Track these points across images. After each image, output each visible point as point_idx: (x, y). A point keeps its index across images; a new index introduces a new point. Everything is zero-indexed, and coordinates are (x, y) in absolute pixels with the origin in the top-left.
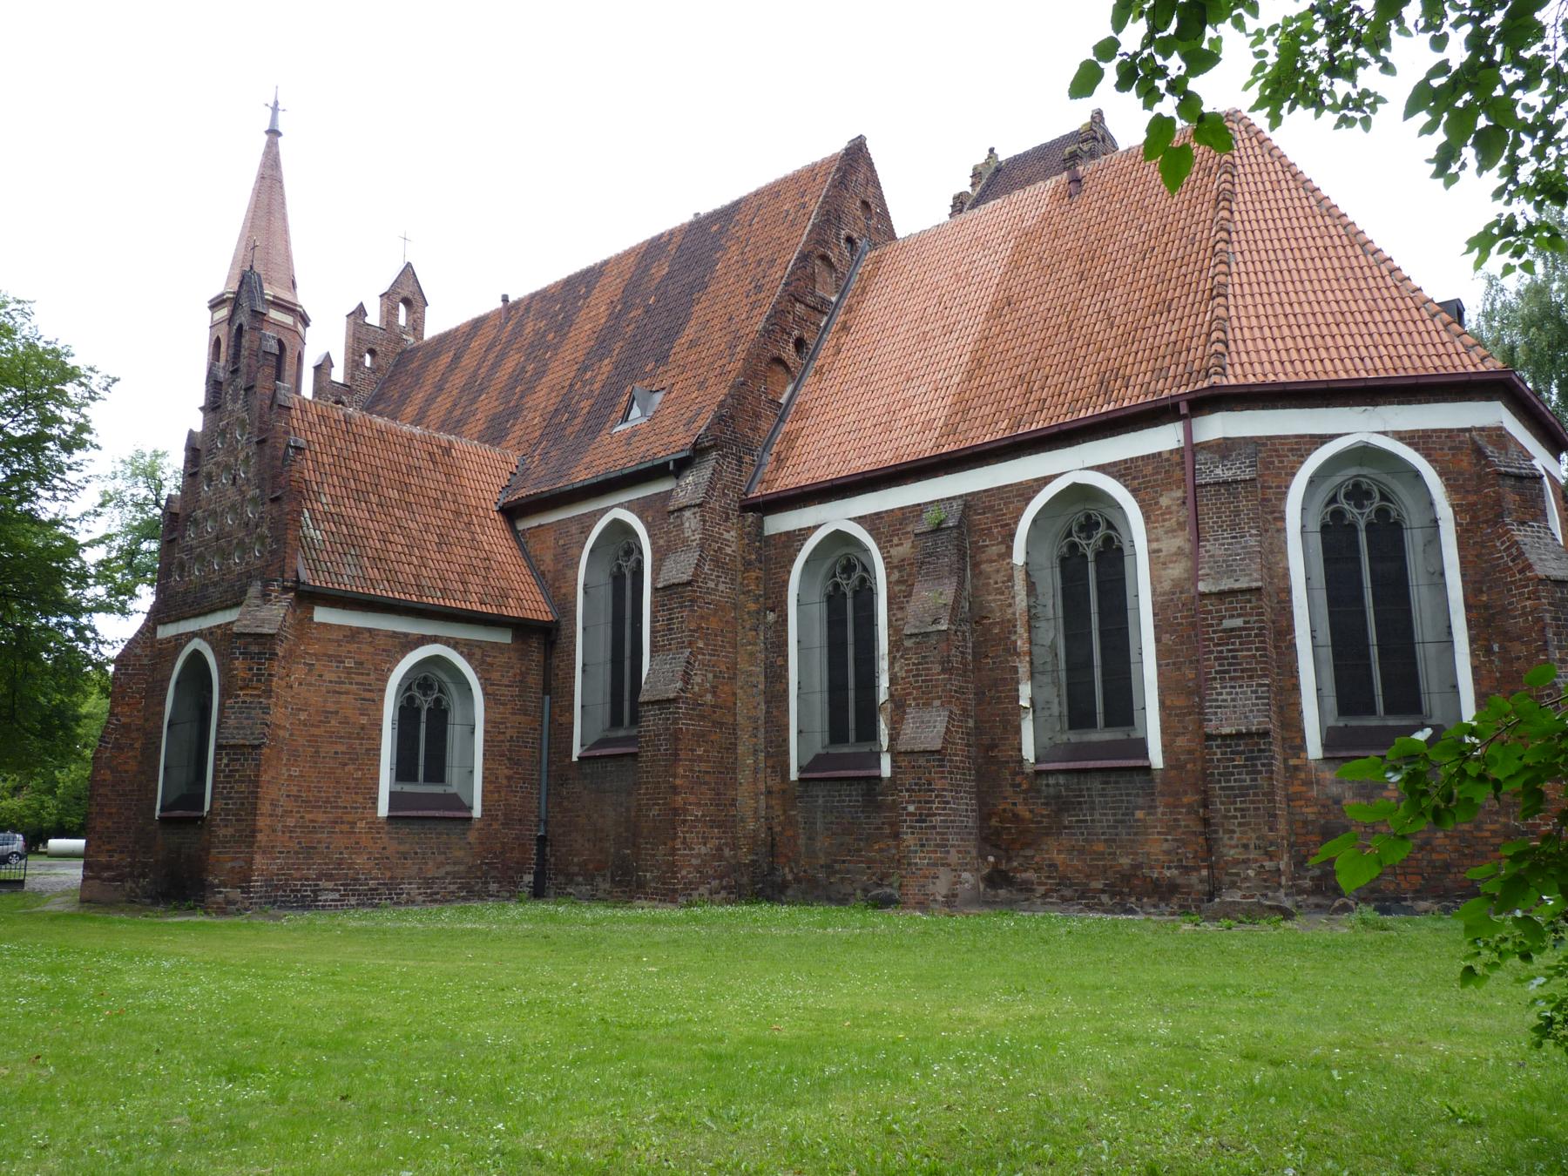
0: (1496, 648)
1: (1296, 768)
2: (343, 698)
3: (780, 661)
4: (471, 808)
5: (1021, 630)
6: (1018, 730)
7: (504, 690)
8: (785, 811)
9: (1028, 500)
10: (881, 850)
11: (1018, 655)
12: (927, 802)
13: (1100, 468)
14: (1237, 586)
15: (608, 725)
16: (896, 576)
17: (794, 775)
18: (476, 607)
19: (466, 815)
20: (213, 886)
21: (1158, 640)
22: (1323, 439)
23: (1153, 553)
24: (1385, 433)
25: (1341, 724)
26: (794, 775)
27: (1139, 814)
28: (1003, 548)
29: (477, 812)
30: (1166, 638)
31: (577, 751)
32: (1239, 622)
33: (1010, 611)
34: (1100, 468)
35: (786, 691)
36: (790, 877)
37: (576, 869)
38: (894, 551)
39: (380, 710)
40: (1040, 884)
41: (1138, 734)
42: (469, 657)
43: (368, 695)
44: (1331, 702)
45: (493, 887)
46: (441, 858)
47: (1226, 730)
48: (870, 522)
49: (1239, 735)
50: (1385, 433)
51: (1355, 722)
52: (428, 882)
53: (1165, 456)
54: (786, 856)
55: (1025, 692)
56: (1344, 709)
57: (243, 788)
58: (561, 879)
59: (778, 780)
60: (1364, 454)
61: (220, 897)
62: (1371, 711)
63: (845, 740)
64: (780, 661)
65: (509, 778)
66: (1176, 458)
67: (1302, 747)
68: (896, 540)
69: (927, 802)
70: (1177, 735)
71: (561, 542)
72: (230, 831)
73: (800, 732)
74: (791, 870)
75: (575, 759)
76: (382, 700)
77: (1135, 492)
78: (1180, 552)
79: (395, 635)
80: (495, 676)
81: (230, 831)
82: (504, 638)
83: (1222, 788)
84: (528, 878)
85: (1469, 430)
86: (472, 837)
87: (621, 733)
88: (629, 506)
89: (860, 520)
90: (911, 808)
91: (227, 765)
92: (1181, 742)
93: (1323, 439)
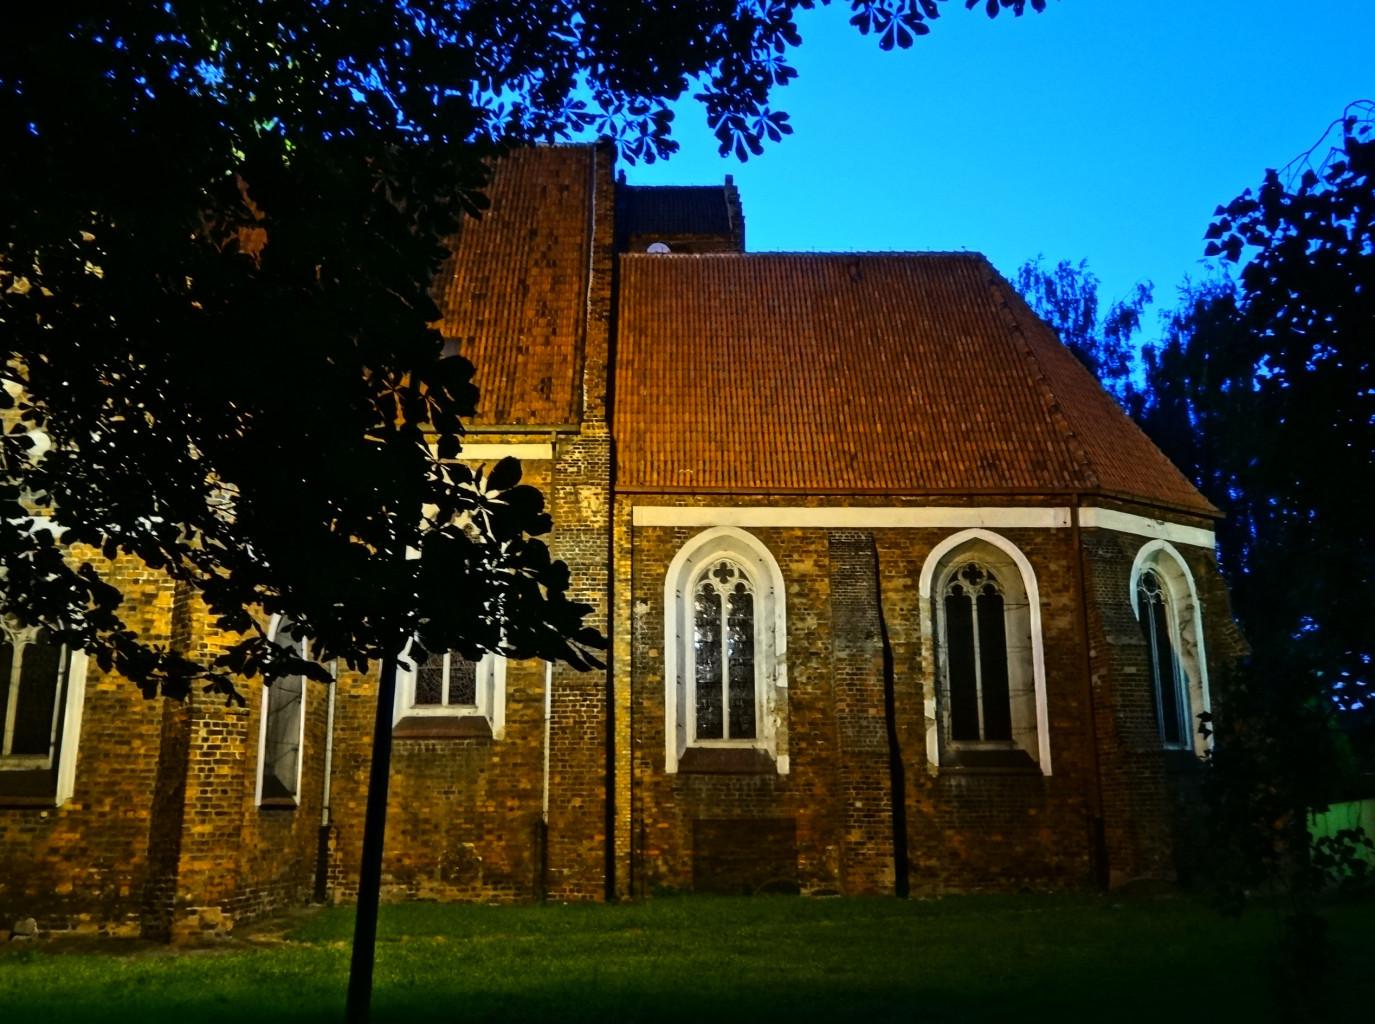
4: (295, 794)
5: (926, 653)
6: (922, 739)
8: (658, 804)
9: (933, 545)
11: (923, 674)
12: (875, 799)
15: (413, 701)
17: (671, 766)
20: (183, 903)
21: (1047, 674)
23: (1044, 606)
26: (671, 766)
27: (1033, 812)
28: (909, 581)
29: (297, 799)
33: (915, 635)
36: (663, 869)
38: (794, 566)
40: (943, 870)
48: (769, 536)
53: (1053, 532)
55: (930, 706)
57: (225, 770)
59: (649, 771)
61: (193, 920)
63: (718, 735)
66: (1061, 535)
68: (796, 556)
69: (875, 799)
72: (207, 828)
74: (666, 862)
77: (1028, 555)
81: (207, 828)
84: (314, 877)
90: (859, 804)
91: (205, 740)
92: (1066, 755)
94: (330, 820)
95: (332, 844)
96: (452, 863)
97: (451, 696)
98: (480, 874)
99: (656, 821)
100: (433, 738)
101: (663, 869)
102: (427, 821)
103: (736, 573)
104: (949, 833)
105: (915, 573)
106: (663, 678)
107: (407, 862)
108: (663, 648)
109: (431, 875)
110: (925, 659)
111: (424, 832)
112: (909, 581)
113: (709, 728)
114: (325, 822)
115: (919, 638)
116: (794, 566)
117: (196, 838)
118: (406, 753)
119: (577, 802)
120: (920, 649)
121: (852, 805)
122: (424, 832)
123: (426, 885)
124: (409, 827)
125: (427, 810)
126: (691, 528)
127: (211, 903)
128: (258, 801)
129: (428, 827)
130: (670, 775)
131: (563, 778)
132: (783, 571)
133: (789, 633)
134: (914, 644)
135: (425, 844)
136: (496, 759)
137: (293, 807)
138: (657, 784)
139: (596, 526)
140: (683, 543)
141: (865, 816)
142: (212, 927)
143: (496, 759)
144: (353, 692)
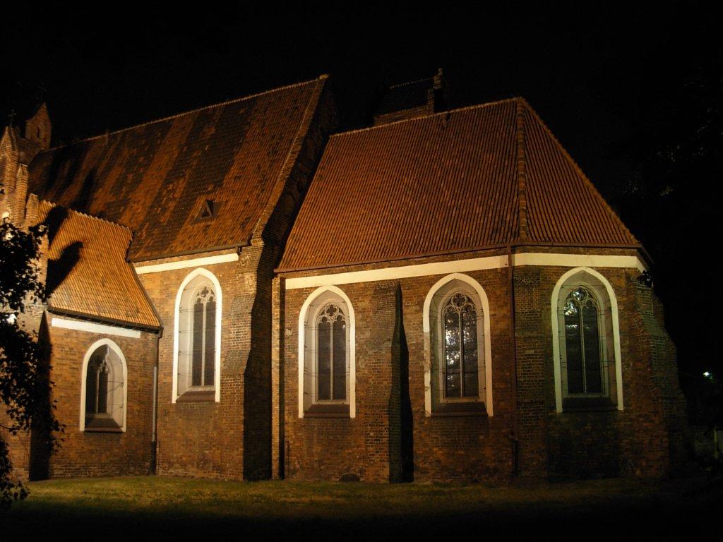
0: (631, 364)
1: (551, 417)
2: (64, 367)
3: (293, 356)
6: (423, 397)
7: (137, 364)
9: (431, 285)
10: (350, 453)
12: (380, 431)
13: (468, 273)
14: (532, 335)
16: (360, 316)
17: (301, 415)
18: (124, 318)
19: (117, 430)
21: (493, 357)
22: (567, 269)
23: (492, 316)
24: (592, 268)
25: (569, 397)
27: (481, 437)
28: (418, 308)
30: (497, 356)
31: (175, 398)
32: (532, 352)
34: (468, 273)
35: (297, 371)
36: (298, 466)
37: (175, 460)
38: (359, 304)
39: (80, 374)
40: (432, 470)
41: (481, 400)
42: (120, 346)
43: (75, 366)
44: (566, 387)
45: (132, 469)
46: (108, 453)
47: (526, 401)
48: (347, 288)
49: (532, 403)
50: (592, 268)
51: (574, 396)
52: (102, 466)
53: (499, 271)
54: (296, 456)
56: (570, 391)
58: (166, 465)
59: (291, 417)
60: (584, 276)
62: (582, 391)
64: (293, 356)
65: (139, 411)
66: (504, 272)
67: (554, 407)
68: (360, 299)
69: (380, 431)
70: (500, 401)
71: (165, 283)
73: (305, 393)
74: (299, 463)
75: (174, 401)
76: (81, 368)
77: (484, 286)
78: (504, 317)
79: (87, 334)
80: (133, 356)
82: (137, 334)
83: (524, 427)
84: (148, 464)
85: (624, 268)
86: (122, 441)
87: (200, 389)
88: (207, 267)
89: (340, 286)
90: (372, 434)
92: (502, 404)
93: (567, 269)
94: (156, 439)
95: (158, 449)
96: (201, 460)
97: (205, 382)
98: (211, 466)
99: (294, 442)
100: (193, 401)
101: (298, 466)
102: (191, 440)
103: (338, 310)
104: (435, 449)
105: (421, 304)
106: (298, 369)
107: (184, 459)
108: (298, 353)
109: (193, 464)
110: (426, 351)
111: (190, 445)
112: (418, 308)
113: (323, 394)
114: (153, 440)
115: (423, 340)
116: (359, 304)
117: (13, 441)
118: (183, 409)
119: (232, 432)
120: (423, 346)
121: (369, 434)
122: (190, 445)
123: (191, 469)
124: (184, 443)
125: (191, 435)
126: (311, 288)
127: (20, 467)
128: (82, 427)
129: (191, 443)
130: (301, 419)
131: (226, 421)
132: (354, 307)
133: (356, 342)
134: (420, 344)
135: (191, 451)
136: (217, 412)
137: (121, 432)
138: (295, 423)
139: (251, 293)
140: (307, 296)
141: (376, 440)
142: (21, 476)
143: (217, 412)
144: (164, 381)
